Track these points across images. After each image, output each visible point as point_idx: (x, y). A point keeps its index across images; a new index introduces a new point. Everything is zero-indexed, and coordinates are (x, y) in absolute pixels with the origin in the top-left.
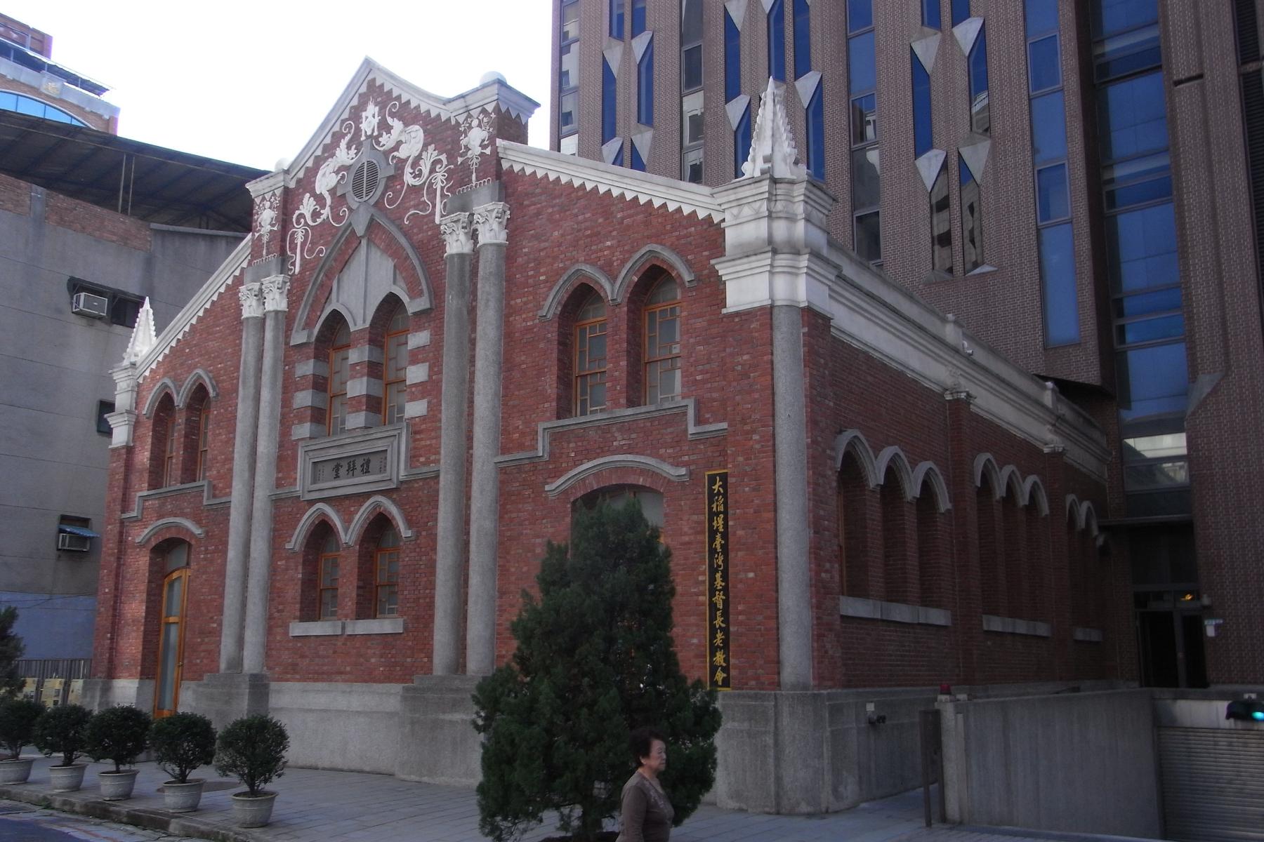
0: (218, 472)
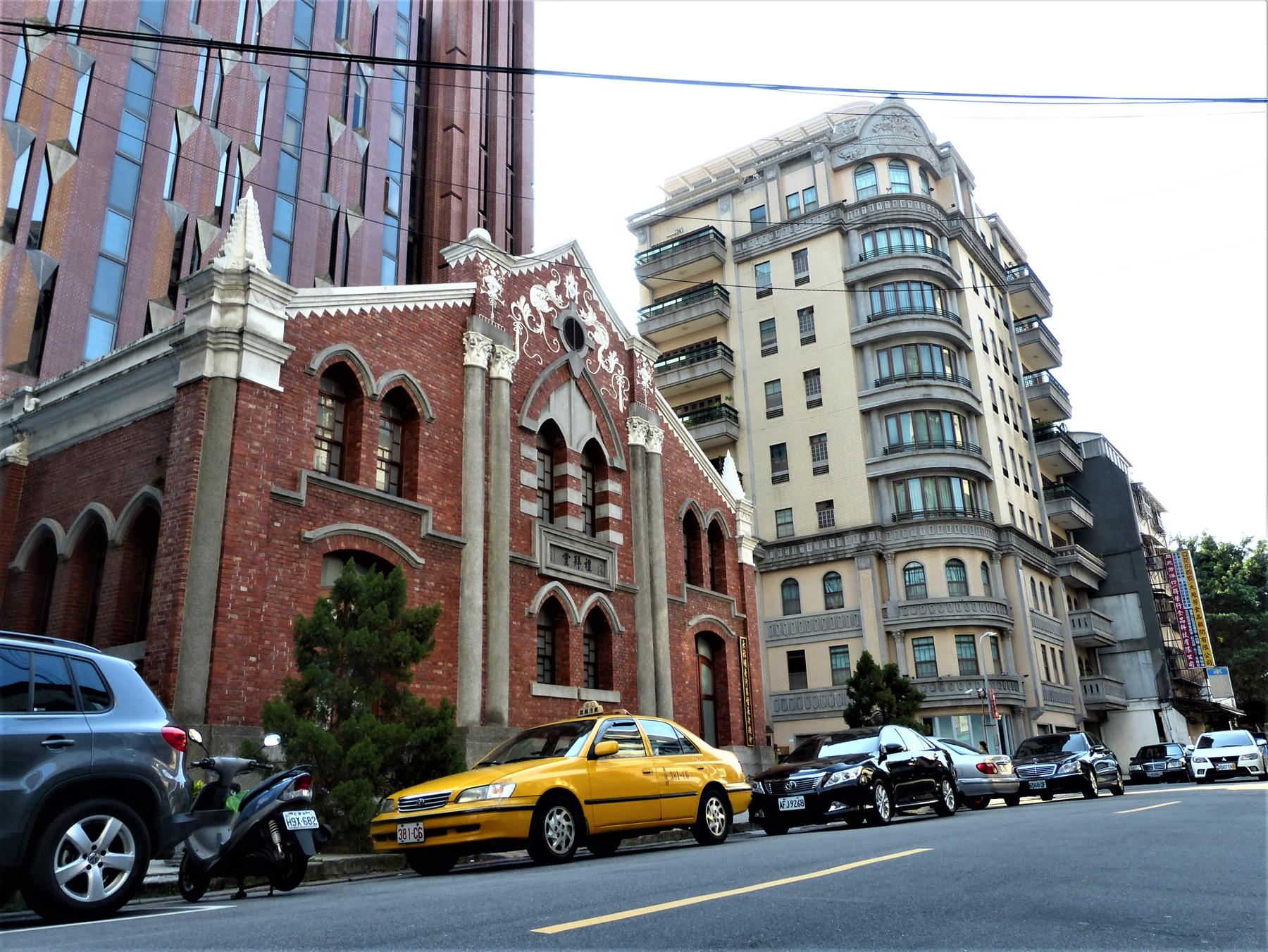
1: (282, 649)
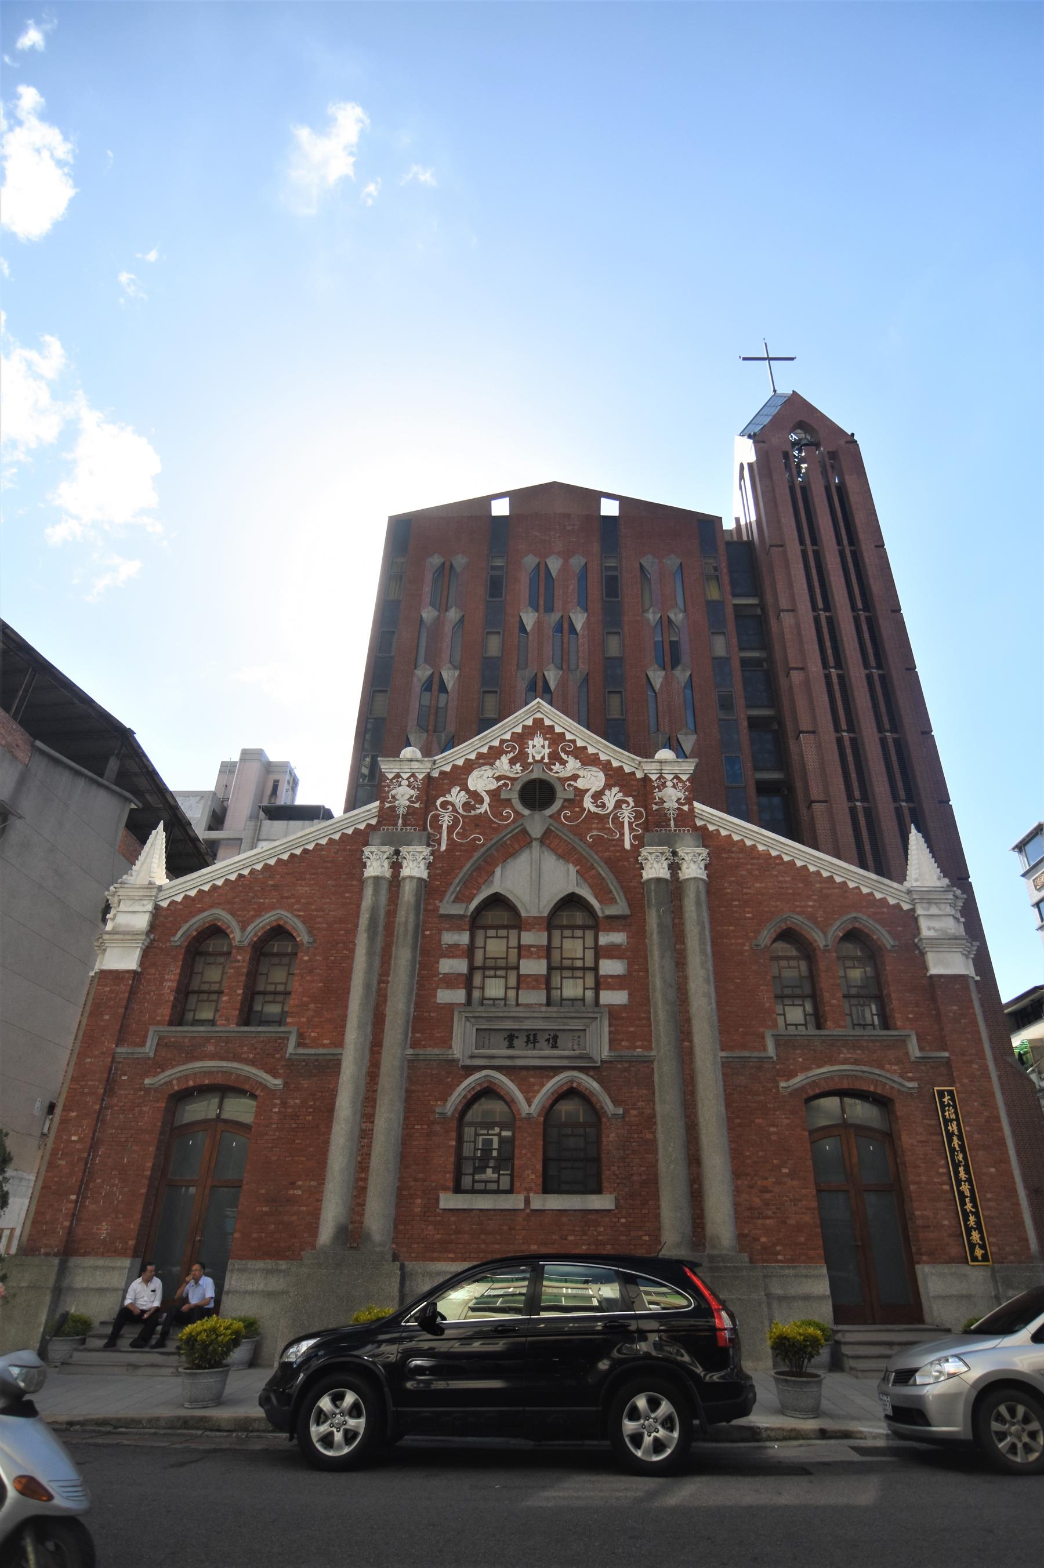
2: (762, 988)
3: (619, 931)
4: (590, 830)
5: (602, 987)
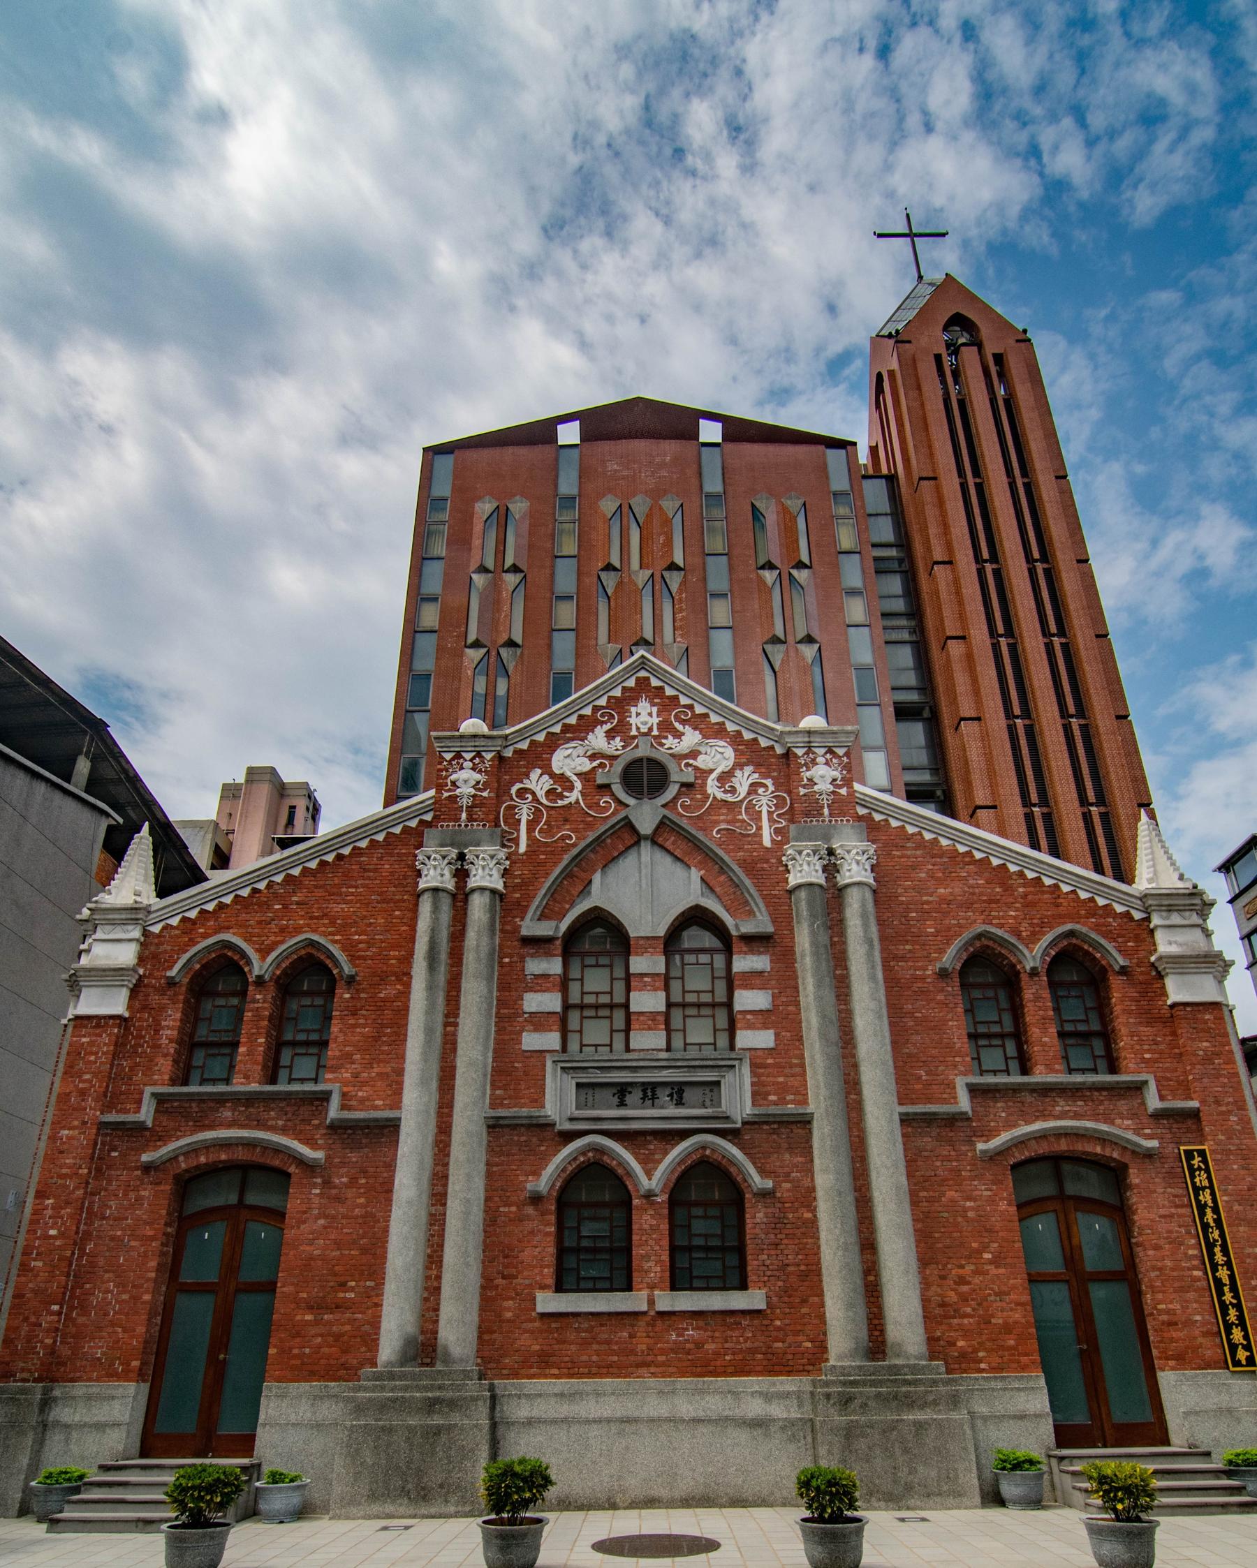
0: (356, 1076)
1: (107, 1291)
2: (950, 1023)
3: (760, 953)
4: (717, 823)
5: (739, 1025)
